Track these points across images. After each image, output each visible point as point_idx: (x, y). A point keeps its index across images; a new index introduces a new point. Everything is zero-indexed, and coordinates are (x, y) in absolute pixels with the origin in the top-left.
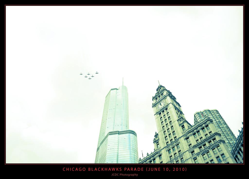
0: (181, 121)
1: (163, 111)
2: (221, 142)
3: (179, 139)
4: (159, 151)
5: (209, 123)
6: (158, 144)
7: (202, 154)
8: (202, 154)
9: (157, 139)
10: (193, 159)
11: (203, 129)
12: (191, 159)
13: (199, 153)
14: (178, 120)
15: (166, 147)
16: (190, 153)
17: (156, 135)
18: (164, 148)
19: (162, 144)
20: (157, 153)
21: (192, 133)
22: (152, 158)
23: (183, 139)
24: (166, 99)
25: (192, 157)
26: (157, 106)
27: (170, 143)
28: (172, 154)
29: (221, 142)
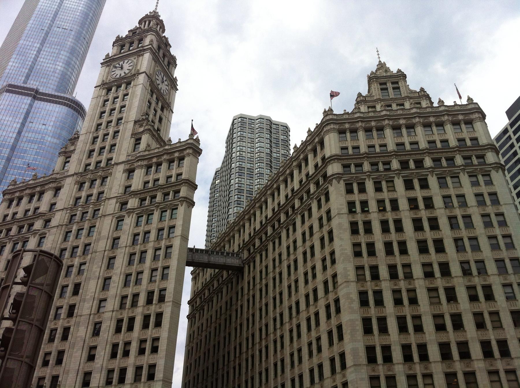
0: (141, 126)
1: (119, 86)
2: (185, 202)
5: (189, 154)
6: (68, 160)
7: (137, 214)
8: (137, 214)
9: (72, 148)
10: (117, 218)
11: (171, 161)
12: (113, 217)
13: (134, 209)
15: (79, 173)
16: (118, 204)
17: (75, 138)
18: (73, 175)
19: (74, 166)
20: (55, 182)
21: (145, 163)
22: (38, 189)
23: (121, 168)
24: (141, 58)
25: (116, 213)
26: (112, 67)
27: (91, 167)
28: (84, 194)
29: (185, 202)
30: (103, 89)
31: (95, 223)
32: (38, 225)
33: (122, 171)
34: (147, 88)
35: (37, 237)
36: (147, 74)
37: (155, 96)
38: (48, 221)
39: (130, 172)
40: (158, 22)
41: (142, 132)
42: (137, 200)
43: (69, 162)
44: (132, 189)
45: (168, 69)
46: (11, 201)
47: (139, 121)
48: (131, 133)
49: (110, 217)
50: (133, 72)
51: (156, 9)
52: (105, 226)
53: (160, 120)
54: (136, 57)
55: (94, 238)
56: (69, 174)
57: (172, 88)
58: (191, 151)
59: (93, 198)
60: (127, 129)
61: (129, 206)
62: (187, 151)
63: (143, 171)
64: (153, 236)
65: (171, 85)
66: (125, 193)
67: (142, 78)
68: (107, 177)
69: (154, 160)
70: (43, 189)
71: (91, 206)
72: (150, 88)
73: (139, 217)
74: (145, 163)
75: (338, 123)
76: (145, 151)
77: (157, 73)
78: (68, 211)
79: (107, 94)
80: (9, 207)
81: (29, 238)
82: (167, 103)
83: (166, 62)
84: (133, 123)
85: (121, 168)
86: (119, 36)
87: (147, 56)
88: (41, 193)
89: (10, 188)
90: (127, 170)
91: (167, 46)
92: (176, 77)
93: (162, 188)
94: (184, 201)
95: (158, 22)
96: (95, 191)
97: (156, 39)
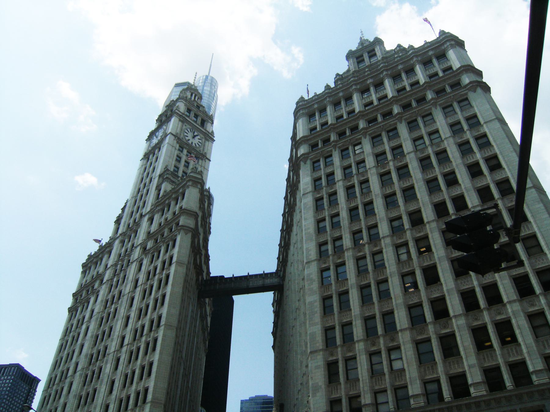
10: (140, 262)
34: (175, 145)
35: (95, 295)
36: (172, 134)
37: (185, 151)
38: (102, 281)
40: (193, 91)
58: (190, 183)
61: (148, 247)
65: (205, 138)
75: (307, 107)
77: (186, 131)
82: (202, 154)
88: (102, 259)
91: (199, 107)
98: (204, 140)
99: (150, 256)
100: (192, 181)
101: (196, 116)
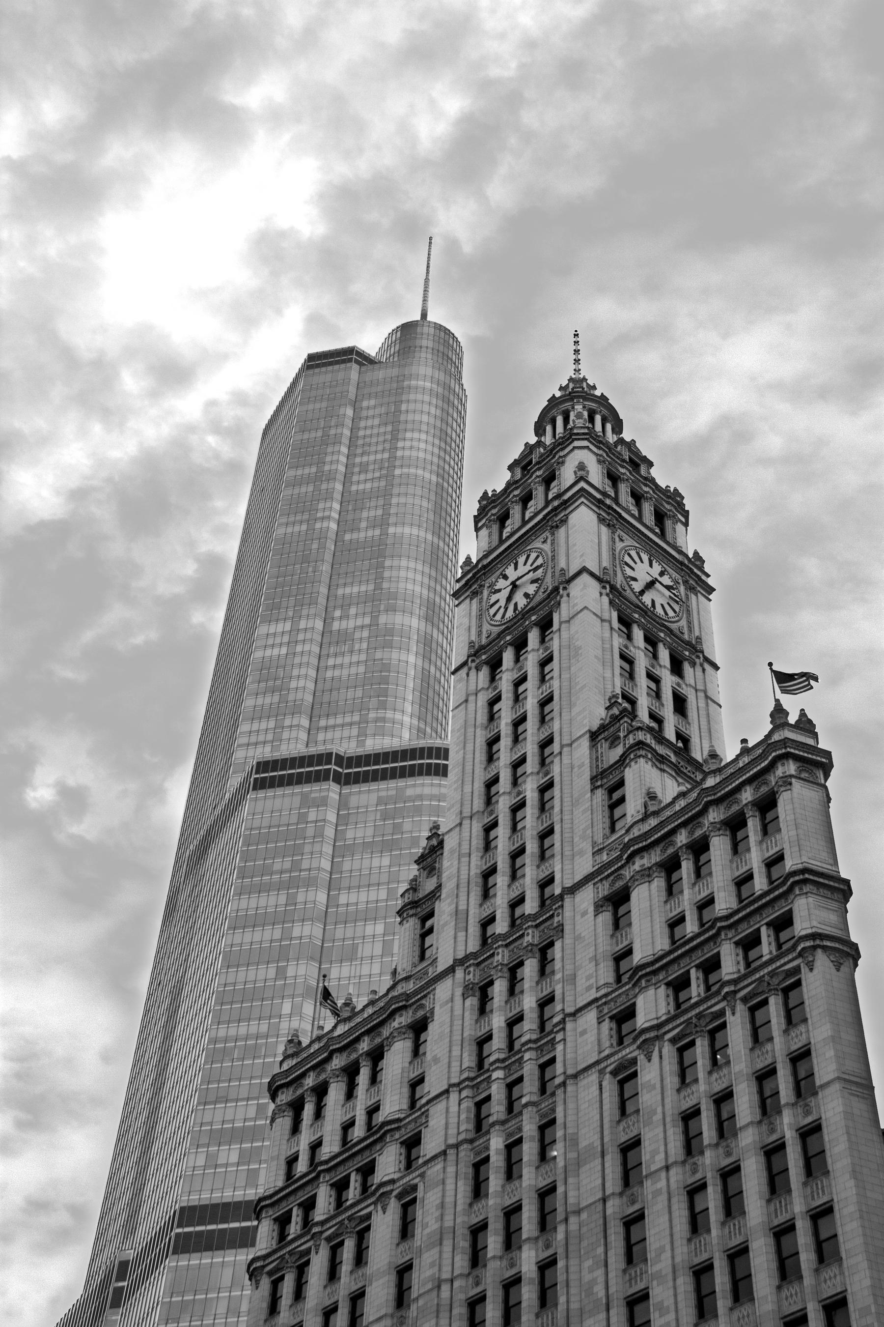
0: (613, 744)
1: (520, 645)
2: (819, 951)
3: (568, 900)
4: (416, 992)
7: (673, 1041)
8: (673, 1041)
9: (429, 885)
10: (614, 1073)
11: (735, 826)
12: (601, 1072)
13: (658, 1026)
14: (594, 736)
15: (467, 957)
16: (606, 1025)
18: (451, 970)
19: (450, 942)
20: (405, 1007)
21: (655, 857)
23: (586, 898)
24: (562, 531)
26: (486, 592)
27: (501, 926)
28: (497, 1022)
29: (819, 951)
30: (478, 669)
31: (553, 1110)
32: (388, 1163)
33: (591, 909)
34: (606, 616)
35: (394, 1207)
36: (592, 574)
37: (638, 635)
38: (413, 1143)
39: (617, 902)
40: (593, 405)
41: (623, 762)
42: (662, 990)
43: (431, 931)
44: (637, 957)
45: (663, 535)
46: (297, 1107)
47: (603, 728)
48: (587, 776)
49: (593, 1077)
50: (549, 583)
51: (577, 371)
52: (586, 1109)
53: (680, 704)
54: (547, 534)
55: (560, 1163)
56: (441, 968)
57: (692, 589)
58: (791, 768)
59: (528, 1028)
60: (575, 764)
61: (642, 1020)
62: (780, 771)
63: (658, 883)
64: (745, 1105)
65: (686, 582)
66: (618, 979)
67: (586, 594)
68: (551, 944)
69: (682, 838)
70: (378, 1040)
71: (527, 1056)
72: (615, 615)
73: (681, 1051)
74: (655, 857)
76: (643, 820)
77: (627, 559)
78: (465, 1093)
79: (493, 679)
80: (295, 1129)
81: (369, 1216)
82: (688, 643)
83: (649, 517)
84: (585, 743)
85: (586, 898)
86: (486, 493)
87: (583, 519)
88: (377, 1056)
89: (285, 1067)
90: (607, 899)
92: (696, 553)
93: (729, 927)
94: (814, 948)
95: (593, 405)
96: (529, 1002)
97: (593, 458)
98: (682, 588)
99: (669, 1051)
100: (796, 758)
101: (637, 498)
